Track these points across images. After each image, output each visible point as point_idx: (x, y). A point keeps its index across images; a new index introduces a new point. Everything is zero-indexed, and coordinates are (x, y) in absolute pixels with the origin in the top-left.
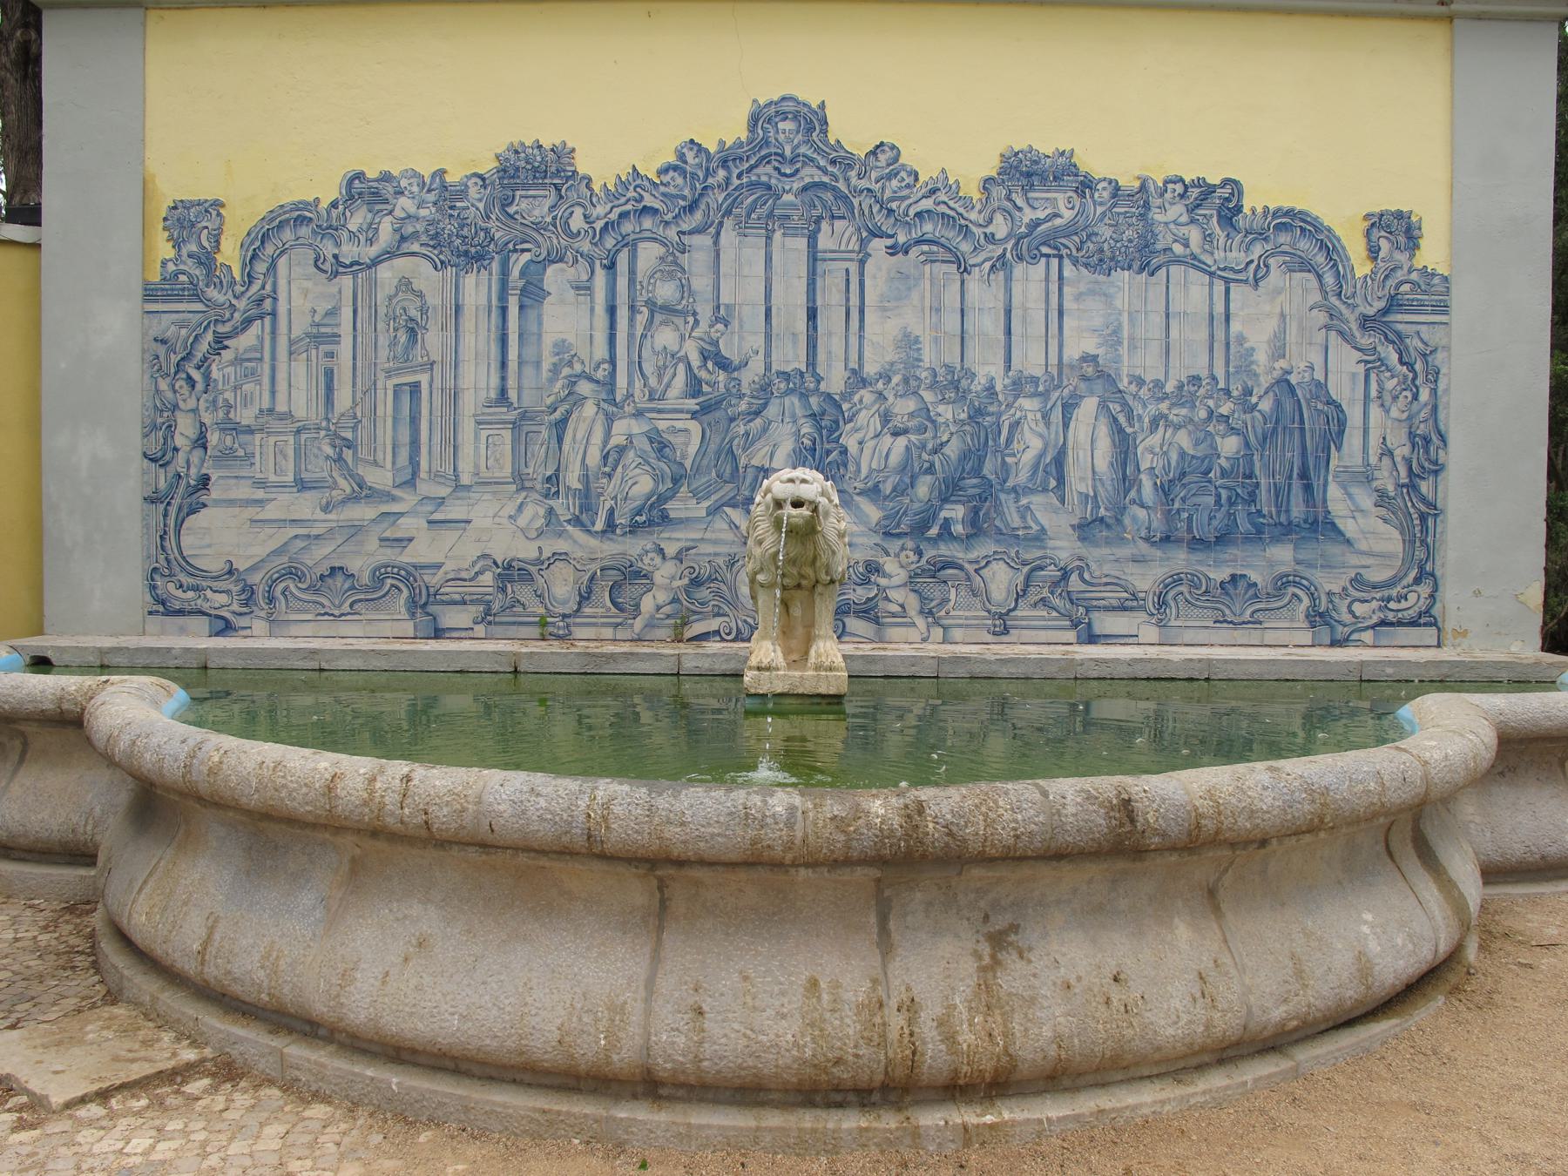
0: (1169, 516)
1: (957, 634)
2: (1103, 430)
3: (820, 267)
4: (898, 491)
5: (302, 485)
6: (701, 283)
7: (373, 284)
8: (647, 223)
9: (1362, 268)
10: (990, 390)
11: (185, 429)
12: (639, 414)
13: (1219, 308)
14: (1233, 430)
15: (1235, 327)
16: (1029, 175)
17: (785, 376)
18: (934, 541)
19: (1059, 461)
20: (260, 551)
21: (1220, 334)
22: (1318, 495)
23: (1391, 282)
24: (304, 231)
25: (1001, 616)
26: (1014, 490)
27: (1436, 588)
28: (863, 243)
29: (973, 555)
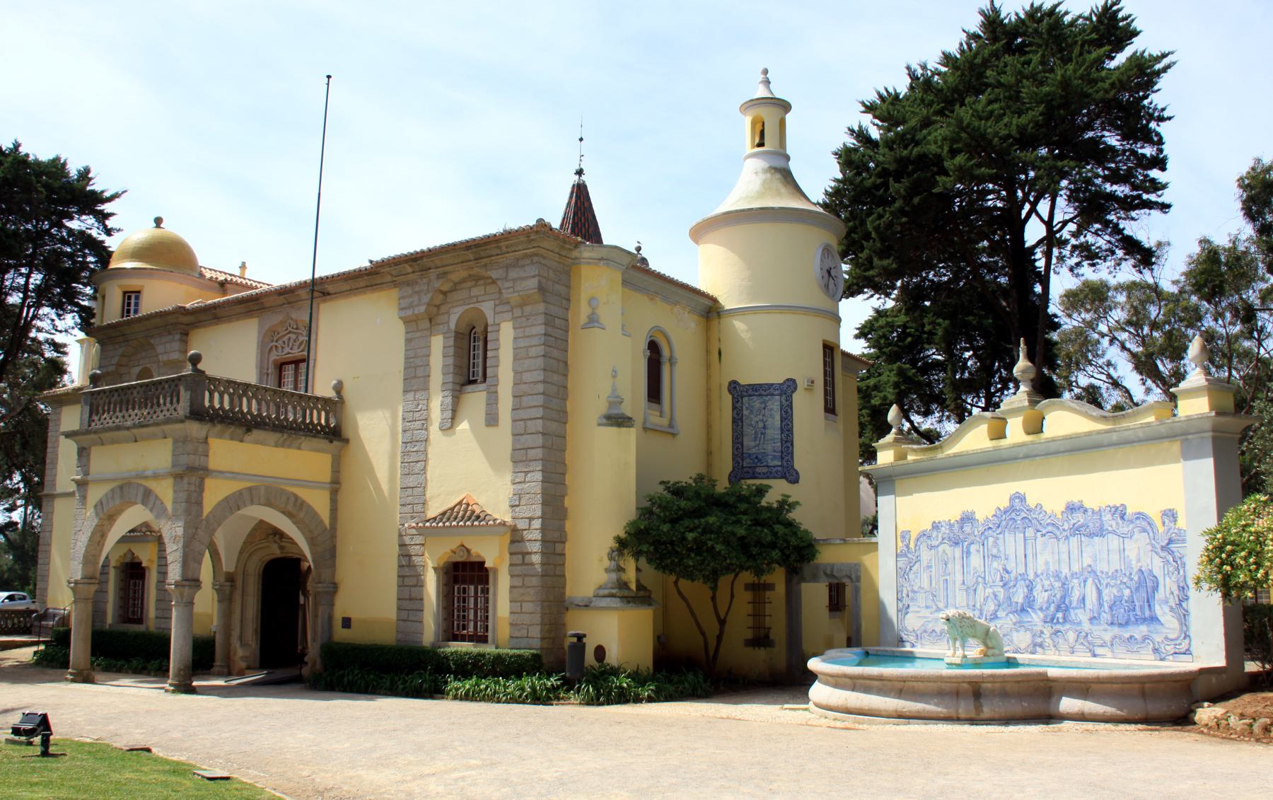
0: (1113, 616)
1: (1062, 653)
2: (1094, 589)
3: (1027, 542)
4: (1047, 608)
5: (927, 607)
6: (1002, 548)
7: (938, 552)
8: (990, 531)
9: (1161, 529)
10: (1066, 577)
11: (905, 592)
12: (991, 587)
13: (1122, 547)
14: (1128, 587)
15: (1126, 552)
16: (1072, 509)
17: (1020, 574)
18: (1055, 624)
19: (1084, 599)
20: (919, 625)
21: (1122, 556)
22: (1152, 607)
23: (1169, 534)
24: (925, 538)
25: (1072, 648)
26: (1073, 608)
27: (1190, 641)
28: (1035, 534)
29: (1064, 628)
